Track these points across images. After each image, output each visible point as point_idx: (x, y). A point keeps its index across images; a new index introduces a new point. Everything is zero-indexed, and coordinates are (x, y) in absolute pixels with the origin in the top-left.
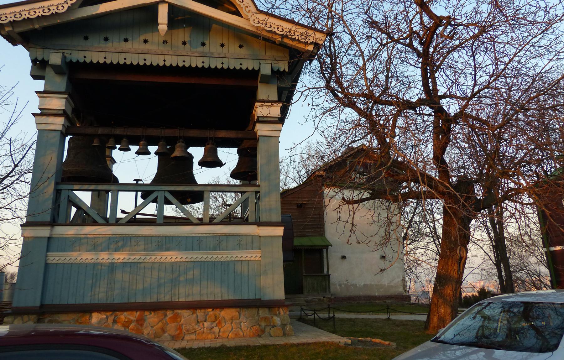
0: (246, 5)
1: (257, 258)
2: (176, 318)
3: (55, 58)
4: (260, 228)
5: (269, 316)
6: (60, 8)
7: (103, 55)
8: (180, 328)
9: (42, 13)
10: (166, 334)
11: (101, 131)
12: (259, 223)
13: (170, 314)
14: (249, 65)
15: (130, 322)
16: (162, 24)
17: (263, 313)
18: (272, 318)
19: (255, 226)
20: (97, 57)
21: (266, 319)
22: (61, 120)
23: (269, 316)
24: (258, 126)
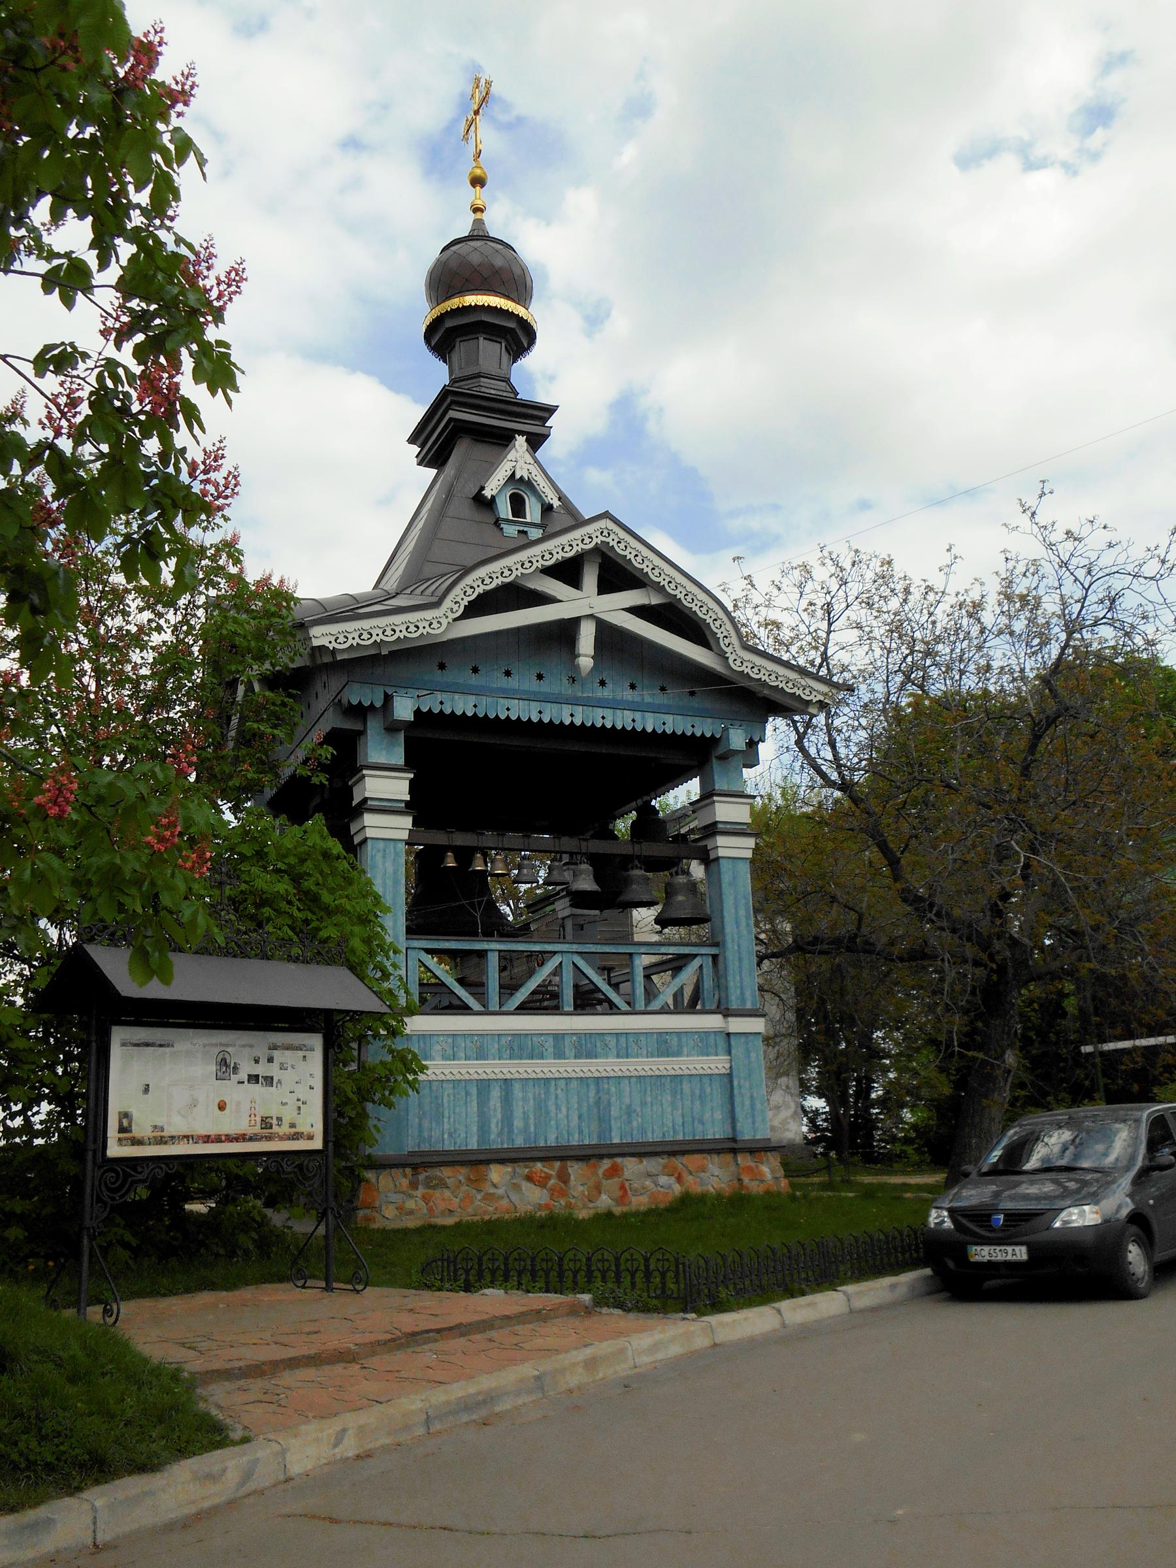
0: (725, 634)
1: (723, 1071)
2: (614, 1171)
3: (404, 709)
4: (730, 1019)
5: (753, 1164)
6: (435, 625)
7: (472, 700)
8: (622, 1187)
9: (405, 633)
10: (604, 1197)
11: (461, 839)
12: (727, 1014)
13: (606, 1164)
14: (704, 728)
15: (548, 1177)
16: (586, 656)
17: (744, 1160)
18: (757, 1167)
19: (720, 1016)
20: (463, 705)
21: (749, 1168)
22: (407, 822)
23: (753, 1164)
24: (721, 840)
